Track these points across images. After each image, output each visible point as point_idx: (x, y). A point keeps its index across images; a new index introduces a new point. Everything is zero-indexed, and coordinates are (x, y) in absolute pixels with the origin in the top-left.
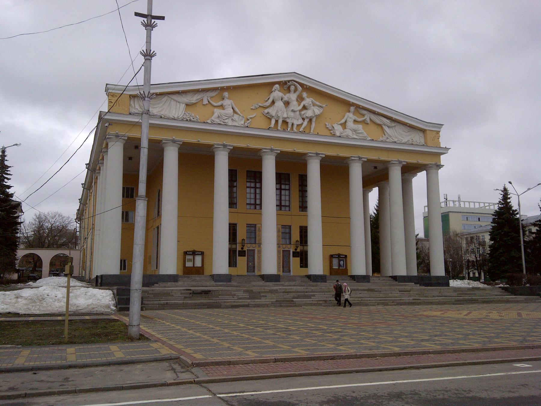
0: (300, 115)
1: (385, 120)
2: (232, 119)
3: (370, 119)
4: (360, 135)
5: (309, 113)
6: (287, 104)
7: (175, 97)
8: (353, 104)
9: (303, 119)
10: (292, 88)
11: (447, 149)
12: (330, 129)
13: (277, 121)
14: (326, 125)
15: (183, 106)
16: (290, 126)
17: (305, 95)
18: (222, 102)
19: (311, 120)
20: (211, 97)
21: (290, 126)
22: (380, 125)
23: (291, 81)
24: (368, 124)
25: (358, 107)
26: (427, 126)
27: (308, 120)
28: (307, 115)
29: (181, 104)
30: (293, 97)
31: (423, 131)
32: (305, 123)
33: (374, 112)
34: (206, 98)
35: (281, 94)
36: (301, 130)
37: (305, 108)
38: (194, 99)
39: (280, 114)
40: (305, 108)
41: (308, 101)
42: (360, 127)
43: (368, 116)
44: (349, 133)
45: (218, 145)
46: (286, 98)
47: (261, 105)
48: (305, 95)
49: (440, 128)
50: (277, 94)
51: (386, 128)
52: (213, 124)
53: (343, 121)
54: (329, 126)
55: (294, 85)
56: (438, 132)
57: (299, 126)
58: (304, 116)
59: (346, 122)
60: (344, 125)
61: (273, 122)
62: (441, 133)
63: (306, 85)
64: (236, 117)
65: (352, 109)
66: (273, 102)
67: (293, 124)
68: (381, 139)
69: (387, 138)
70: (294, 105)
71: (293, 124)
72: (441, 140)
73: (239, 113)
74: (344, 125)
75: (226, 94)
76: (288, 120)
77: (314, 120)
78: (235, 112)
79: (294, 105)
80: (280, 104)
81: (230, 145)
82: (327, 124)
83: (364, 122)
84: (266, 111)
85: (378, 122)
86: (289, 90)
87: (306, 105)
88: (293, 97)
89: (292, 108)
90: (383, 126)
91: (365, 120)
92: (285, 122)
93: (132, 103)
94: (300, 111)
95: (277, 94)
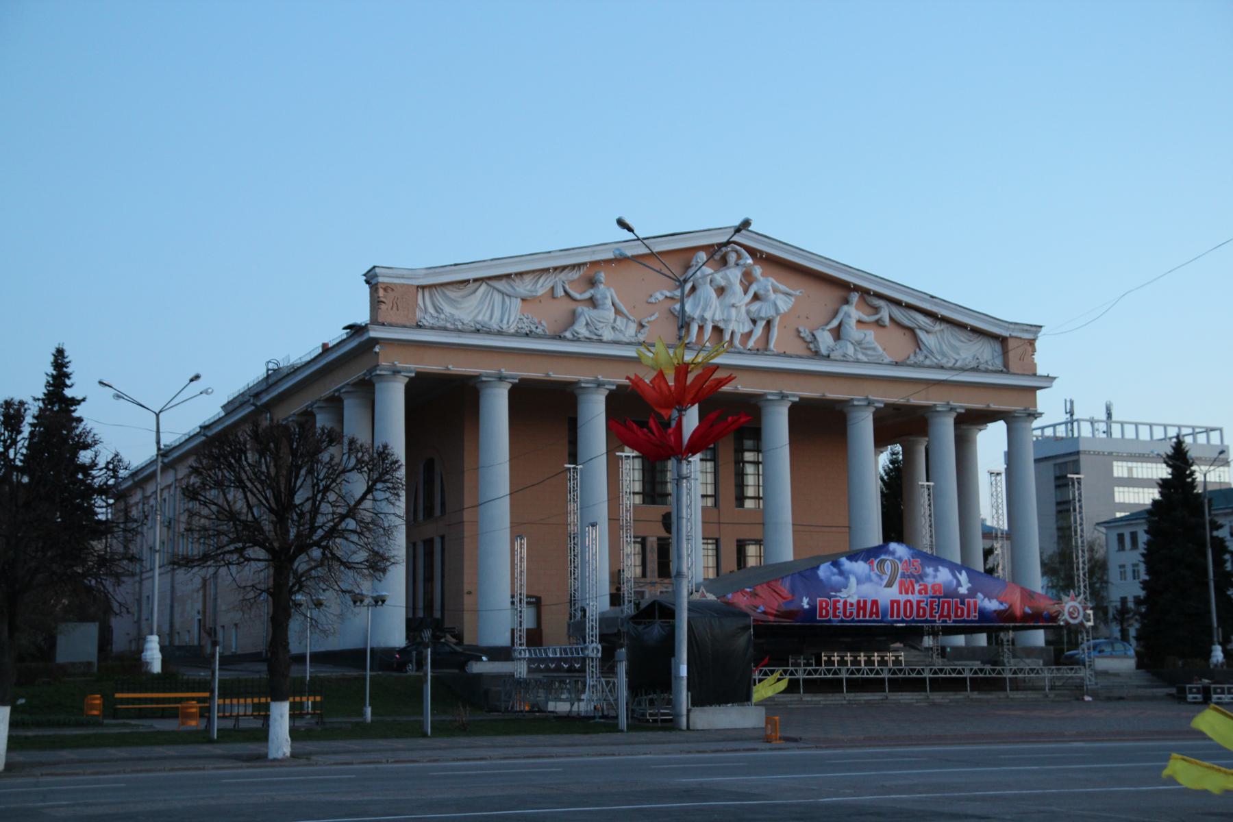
0: (748, 312)
1: (921, 319)
2: (613, 328)
3: (891, 318)
4: (869, 352)
5: (765, 310)
6: (721, 291)
7: (502, 285)
8: (857, 288)
9: (754, 322)
10: (732, 258)
11: (1050, 379)
12: (808, 339)
13: (701, 328)
14: (799, 332)
17: (758, 271)
18: (592, 291)
19: (769, 323)
20: (571, 282)
21: (727, 337)
22: (911, 330)
24: (884, 326)
25: (865, 292)
26: (1008, 329)
27: (764, 323)
28: (763, 315)
29: (514, 300)
31: (1003, 340)
32: (759, 331)
33: (897, 303)
36: (751, 344)
39: (708, 315)
40: (756, 297)
42: (870, 335)
43: (885, 312)
45: (587, 382)
46: (719, 278)
47: (668, 294)
49: (1036, 333)
52: (576, 339)
53: (835, 323)
54: (805, 333)
55: (736, 252)
56: (1032, 342)
58: (755, 316)
59: (840, 325)
62: (1038, 344)
63: (761, 252)
64: (620, 322)
65: (855, 297)
68: (912, 360)
69: (926, 357)
71: (733, 333)
72: (1038, 358)
73: (625, 311)
74: (837, 333)
76: (721, 325)
77: (777, 322)
78: (618, 312)
81: (610, 383)
82: (801, 329)
83: (879, 324)
86: (724, 262)
87: (762, 292)
89: (733, 301)
90: (918, 332)
92: (717, 330)
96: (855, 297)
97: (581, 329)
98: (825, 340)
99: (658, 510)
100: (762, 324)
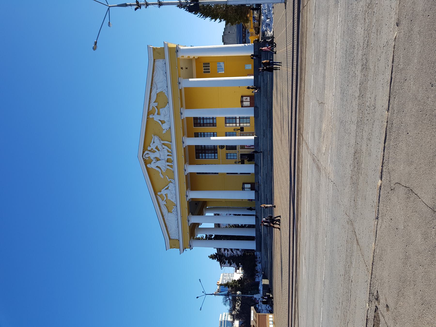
6: (158, 159)
10: (147, 156)
15: (170, 214)
16: (169, 157)
23: (143, 159)
28: (161, 147)
30: (152, 156)
34: (162, 203)
35: (152, 163)
36: (170, 150)
37: (157, 148)
38: (165, 210)
41: (153, 147)
43: (153, 104)
44: (167, 117)
46: (154, 161)
48: (149, 148)
50: (152, 166)
51: (158, 91)
54: (164, 132)
56: (154, 49)
57: (168, 151)
60: (163, 122)
61: (168, 167)
66: (157, 167)
67: (168, 155)
70: (157, 154)
71: (168, 155)
74: (163, 122)
75: (159, 193)
77: (163, 142)
79: (157, 154)
80: (159, 164)
84: (163, 170)
85: (155, 97)
86: (149, 157)
88: (152, 156)
91: (156, 107)
92: (168, 161)
93: (173, 238)
94: (159, 150)
95: (152, 166)
96: (151, 116)
97: (173, 200)
98: (165, 126)
99: (219, 150)
100: (164, 146)
